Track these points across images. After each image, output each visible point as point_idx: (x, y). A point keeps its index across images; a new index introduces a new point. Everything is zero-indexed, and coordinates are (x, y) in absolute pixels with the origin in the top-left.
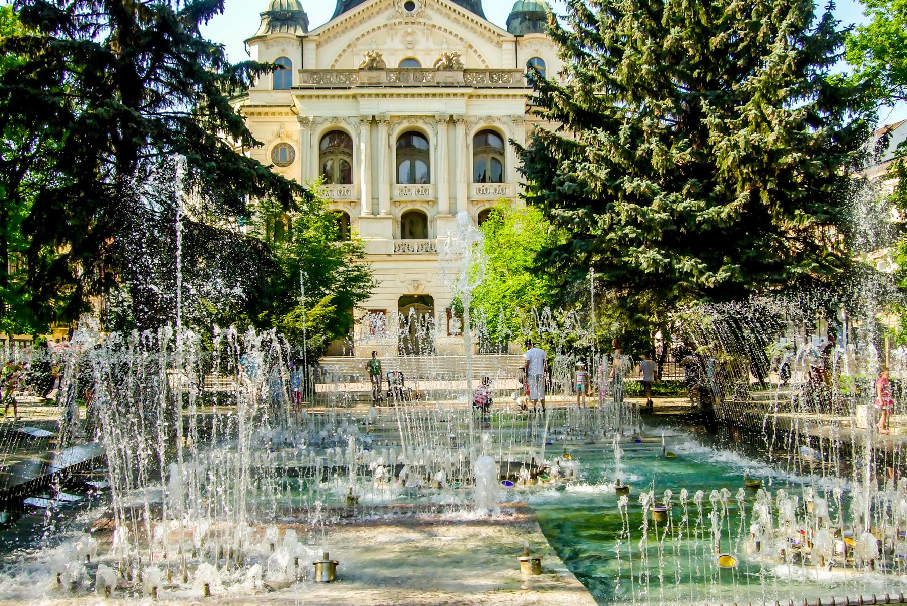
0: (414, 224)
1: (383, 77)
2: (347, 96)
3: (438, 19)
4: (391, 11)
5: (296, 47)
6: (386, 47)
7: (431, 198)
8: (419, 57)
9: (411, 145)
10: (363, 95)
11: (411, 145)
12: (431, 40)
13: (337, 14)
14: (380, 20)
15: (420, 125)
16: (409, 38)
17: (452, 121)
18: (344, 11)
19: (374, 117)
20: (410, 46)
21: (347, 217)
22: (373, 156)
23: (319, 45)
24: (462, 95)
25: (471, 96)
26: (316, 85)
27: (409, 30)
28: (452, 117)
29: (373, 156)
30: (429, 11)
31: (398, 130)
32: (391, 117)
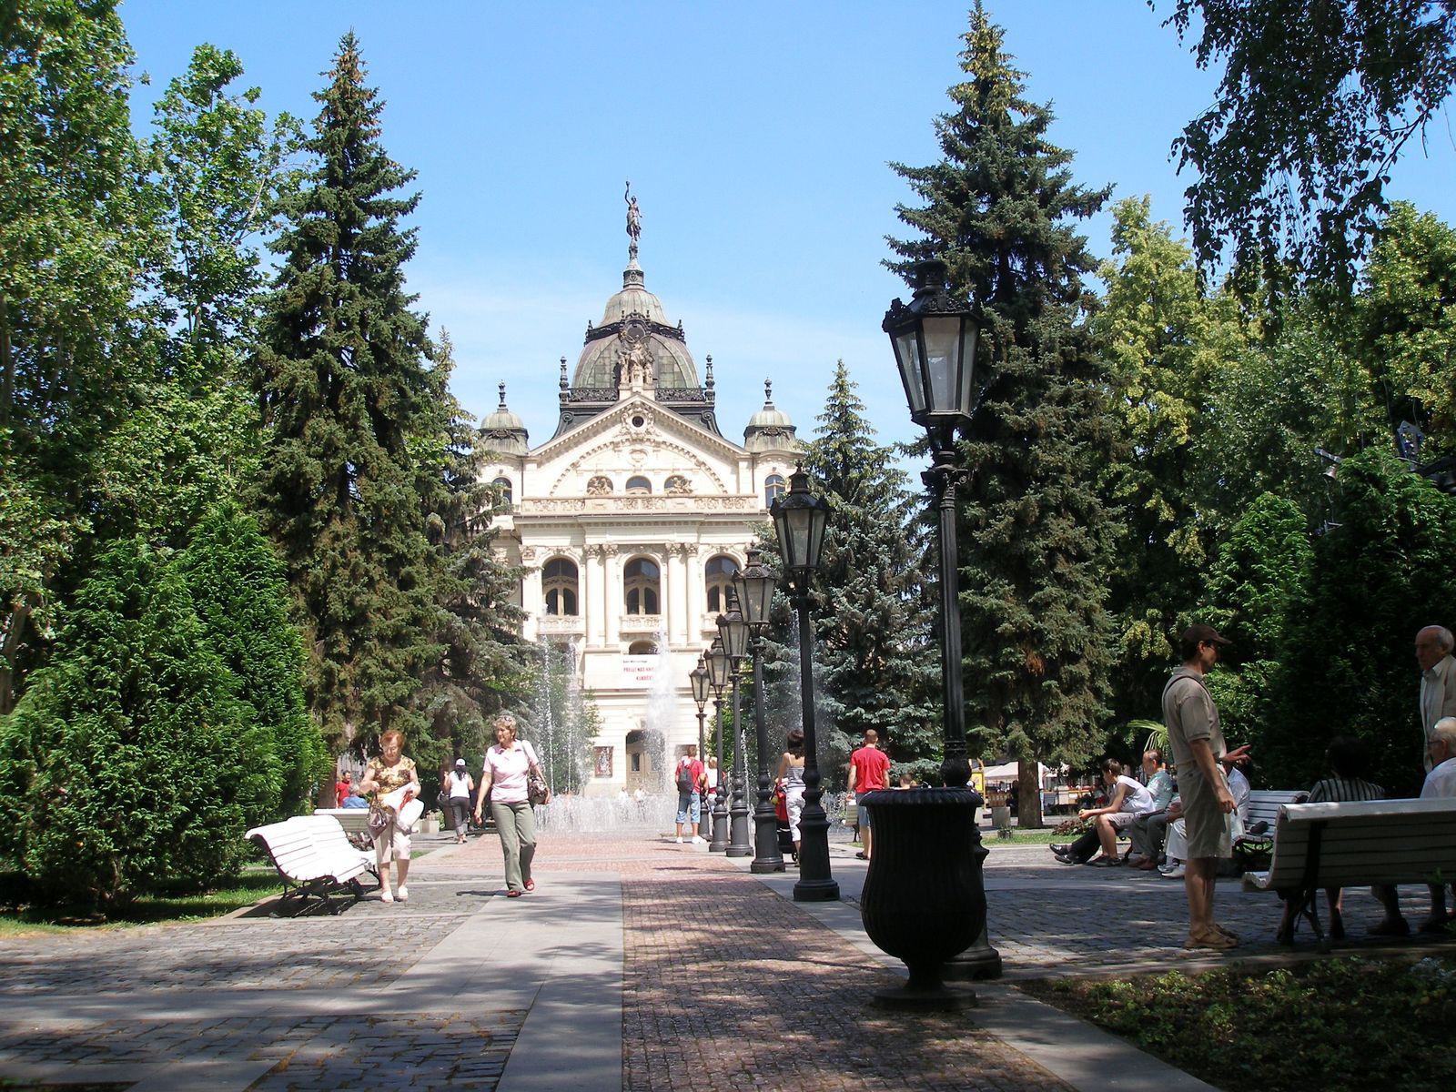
1: (611, 508)
2: (572, 525)
3: (665, 436)
4: (618, 427)
8: (649, 476)
10: (589, 524)
13: (557, 434)
16: (637, 456)
17: (685, 551)
19: (601, 546)
20: (638, 465)
22: (602, 585)
23: (540, 464)
24: (694, 522)
25: (702, 523)
26: (539, 514)
28: (683, 545)
29: (602, 585)
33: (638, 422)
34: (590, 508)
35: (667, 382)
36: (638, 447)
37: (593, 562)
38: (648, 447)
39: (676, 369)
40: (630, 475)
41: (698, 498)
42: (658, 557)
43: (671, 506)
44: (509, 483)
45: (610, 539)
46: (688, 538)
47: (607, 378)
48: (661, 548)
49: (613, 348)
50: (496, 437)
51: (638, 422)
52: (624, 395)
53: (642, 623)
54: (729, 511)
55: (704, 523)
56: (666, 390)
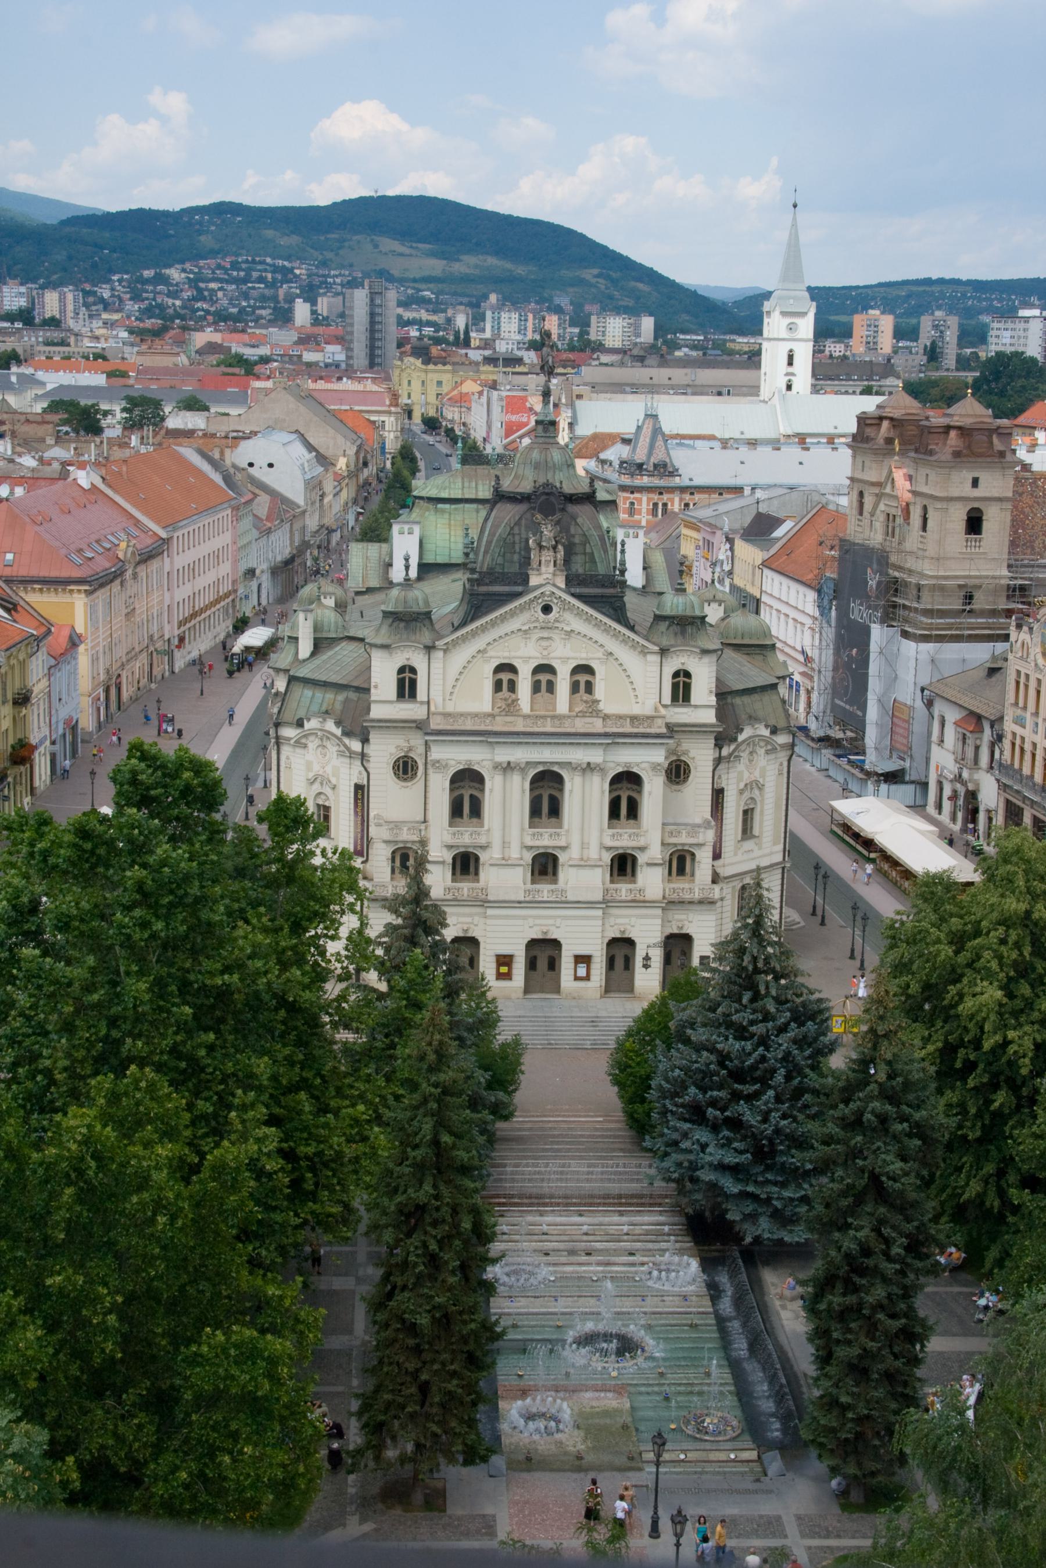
0: (545, 866)
3: (576, 624)
4: (525, 616)
5: (421, 656)
6: (518, 654)
7: (563, 843)
8: (555, 664)
9: (546, 796)
11: (546, 796)
12: (568, 646)
14: (515, 624)
15: (556, 769)
16: (545, 643)
18: (473, 619)
20: (545, 653)
21: (477, 859)
23: (445, 651)
27: (545, 634)
28: (589, 764)
30: (568, 616)
31: (532, 773)
32: (527, 763)
33: (547, 609)
34: (499, 725)
35: (579, 566)
36: (545, 634)
37: (498, 779)
38: (556, 636)
39: (588, 550)
40: (534, 664)
41: (606, 717)
42: (564, 773)
43: (580, 725)
44: (413, 670)
45: (520, 754)
46: (595, 756)
47: (516, 557)
48: (568, 765)
49: (523, 522)
50: (401, 620)
51: (547, 609)
52: (534, 581)
53: (545, 839)
54: (635, 730)
55: (613, 739)
56: (578, 576)
